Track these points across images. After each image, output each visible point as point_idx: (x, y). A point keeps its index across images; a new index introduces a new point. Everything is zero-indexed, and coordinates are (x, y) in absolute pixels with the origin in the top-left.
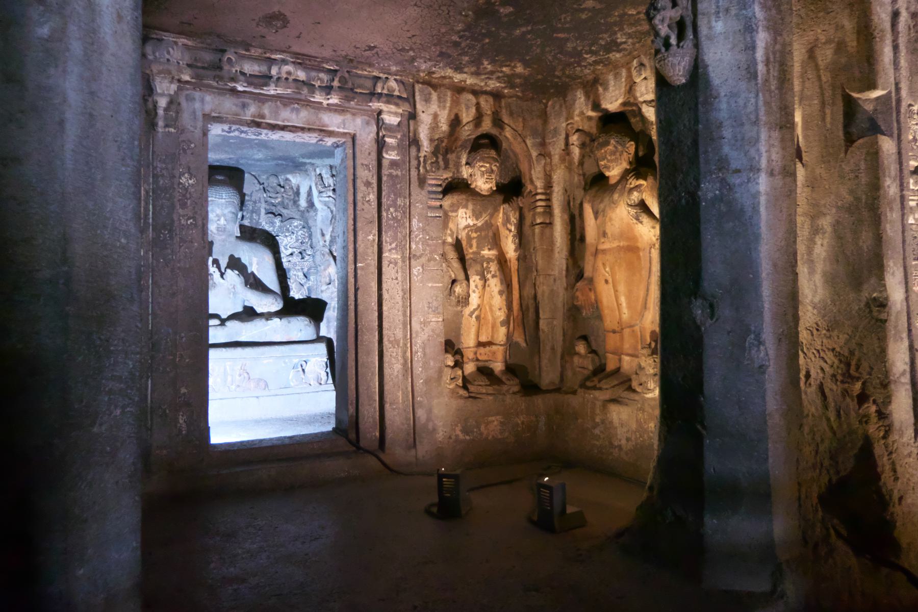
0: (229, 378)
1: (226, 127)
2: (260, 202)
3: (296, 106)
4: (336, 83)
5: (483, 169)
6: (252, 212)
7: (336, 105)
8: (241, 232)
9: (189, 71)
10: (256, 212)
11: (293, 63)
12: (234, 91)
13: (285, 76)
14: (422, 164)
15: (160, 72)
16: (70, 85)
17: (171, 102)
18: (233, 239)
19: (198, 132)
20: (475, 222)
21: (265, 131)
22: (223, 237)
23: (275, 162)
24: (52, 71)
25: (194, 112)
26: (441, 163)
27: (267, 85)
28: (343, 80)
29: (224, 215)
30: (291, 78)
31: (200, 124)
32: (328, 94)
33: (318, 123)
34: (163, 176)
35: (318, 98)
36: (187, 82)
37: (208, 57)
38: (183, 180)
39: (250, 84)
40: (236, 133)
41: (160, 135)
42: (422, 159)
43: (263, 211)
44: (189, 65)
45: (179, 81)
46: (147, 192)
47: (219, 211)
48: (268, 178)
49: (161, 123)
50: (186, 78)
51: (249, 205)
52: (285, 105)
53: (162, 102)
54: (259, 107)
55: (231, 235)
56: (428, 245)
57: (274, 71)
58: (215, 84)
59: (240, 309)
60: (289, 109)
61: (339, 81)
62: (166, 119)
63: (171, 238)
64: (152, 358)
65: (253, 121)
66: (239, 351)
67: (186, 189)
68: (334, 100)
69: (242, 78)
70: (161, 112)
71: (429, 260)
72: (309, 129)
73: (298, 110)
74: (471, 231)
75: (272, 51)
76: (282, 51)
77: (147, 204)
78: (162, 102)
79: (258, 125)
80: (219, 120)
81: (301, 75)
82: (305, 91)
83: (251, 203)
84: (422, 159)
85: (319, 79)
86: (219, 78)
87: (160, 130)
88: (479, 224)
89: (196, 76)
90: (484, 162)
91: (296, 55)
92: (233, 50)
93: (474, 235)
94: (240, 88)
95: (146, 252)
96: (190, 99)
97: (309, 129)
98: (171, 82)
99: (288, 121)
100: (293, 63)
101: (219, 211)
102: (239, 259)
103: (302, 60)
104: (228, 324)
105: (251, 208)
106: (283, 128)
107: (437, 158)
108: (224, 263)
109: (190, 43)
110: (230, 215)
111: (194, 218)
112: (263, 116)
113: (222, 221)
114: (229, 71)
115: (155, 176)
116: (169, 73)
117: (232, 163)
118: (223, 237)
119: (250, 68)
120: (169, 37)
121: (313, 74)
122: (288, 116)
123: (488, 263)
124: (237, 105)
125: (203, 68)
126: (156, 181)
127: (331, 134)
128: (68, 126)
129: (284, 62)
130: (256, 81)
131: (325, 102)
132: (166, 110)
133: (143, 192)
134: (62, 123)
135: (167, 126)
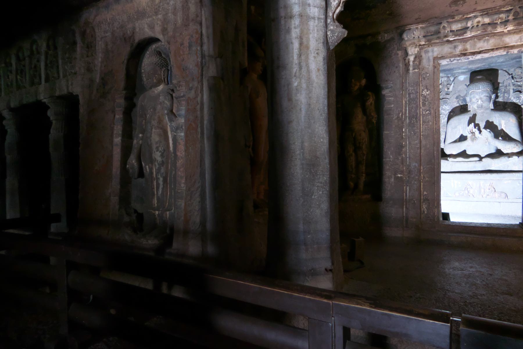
0: (482, 190)
1: (448, 60)
2: (509, 86)
3: (487, 38)
4: (511, 17)
6: (504, 92)
7: (513, 30)
8: (494, 107)
9: (424, 40)
10: (506, 93)
11: (481, 15)
12: (448, 41)
13: (476, 25)
15: (410, 45)
16: (302, 98)
17: (415, 58)
18: (489, 111)
19: (431, 68)
21: (470, 57)
22: (482, 111)
23: (514, 61)
24: (298, 95)
25: (429, 58)
27: (465, 33)
28: (516, 14)
29: (481, 99)
30: (480, 24)
31: (431, 63)
32: (505, 26)
33: (501, 44)
34: (412, 93)
35: (499, 29)
36: (424, 45)
37: (433, 29)
38: (424, 93)
39: (456, 36)
40: (455, 61)
41: (411, 74)
43: (512, 91)
44: (424, 37)
45: (420, 45)
46: (406, 102)
47: (477, 97)
48: (515, 70)
49: (411, 68)
50: (423, 43)
51: (502, 89)
52: (480, 40)
53: (412, 58)
54: (464, 45)
55: (487, 109)
57: (469, 24)
58: (438, 41)
59: (493, 151)
60: (482, 41)
61: (513, 15)
62: (413, 66)
63: (417, 122)
64: (409, 177)
65: (461, 54)
66: (489, 175)
67: (425, 97)
68: (510, 27)
69: (451, 34)
70: (411, 63)
72: (497, 49)
73: (488, 40)
75: (467, 14)
76: (473, 12)
77: (406, 107)
78: (412, 58)
79: (465, 55)
80: (443, 58)
81: (487, 20)
82: (490, 28)
83: (503, 87)
85: (500, 18)
86: (439, 38)
87: (411, 72)
89: (429, 41)
91: (482, 11)
92: (445, 21)
94: (451, 39)
95: (406, 130)
96: (427, 52)
97: (497, 49)
98: (416, 48)
99: (482, 48)
100: (481, 15)
101: (477, 97)
102: (493, 122)
103: (486, 12)
104: (483, 160)
105: (503, 90)
106: (480, 52)
108: (482, 125)
109: (423, 26)
110: (485, 98)
111: (429, 110)
112: (466, 50)
113: (480, 102)
114: (444, 33)
115: (409, 94)
116: (414, 43)
117: (487, 67)
118: (482, 111)
119: (456, 27)
120: (413, 27)
121: (496, 17)
122: (482, 45)
124: (451, 48)
125: (432, 35)
126: (409, 96)
127: (513, 47)
128: (302, 109)
129: (476, 17)
130: (459, 33)
131: (506, 31)
132: (414, 61)
133: (404, 102)
134: (300, 109)
135: (414, 69)
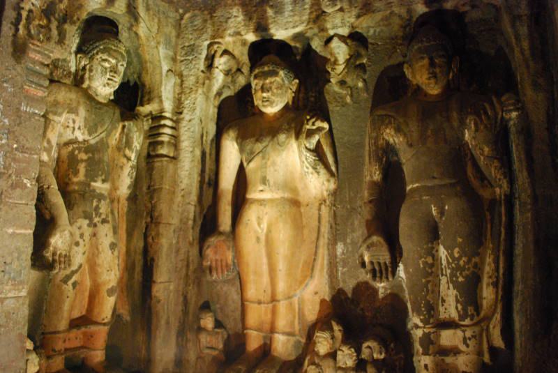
5: (107, 65)
14: (23, 21)
20: (87, 137)
26: (55, 32)
42: (24, 14)
56: (14, 160)
71: (13, 186)
74: (79, 149)
84: (24, 14)
88: (93, 142)
90: (110, 55)
93: (83, 156)
107: (49, 21)
123: (99, 201)
